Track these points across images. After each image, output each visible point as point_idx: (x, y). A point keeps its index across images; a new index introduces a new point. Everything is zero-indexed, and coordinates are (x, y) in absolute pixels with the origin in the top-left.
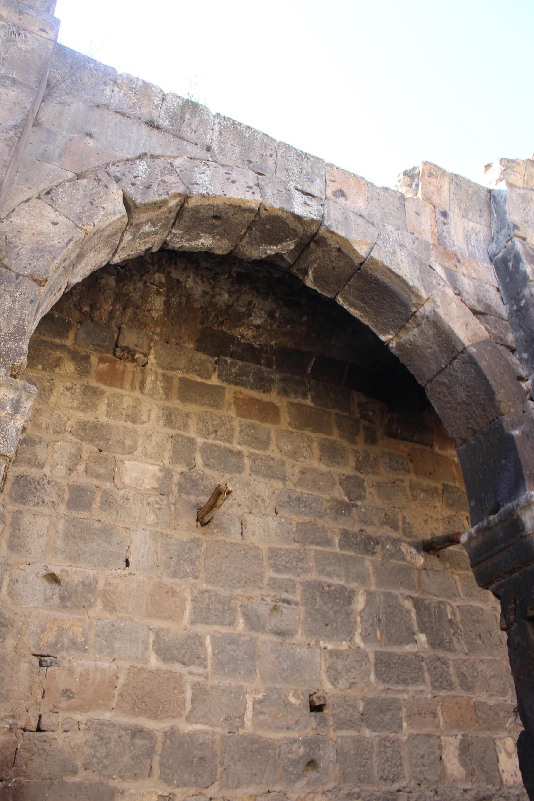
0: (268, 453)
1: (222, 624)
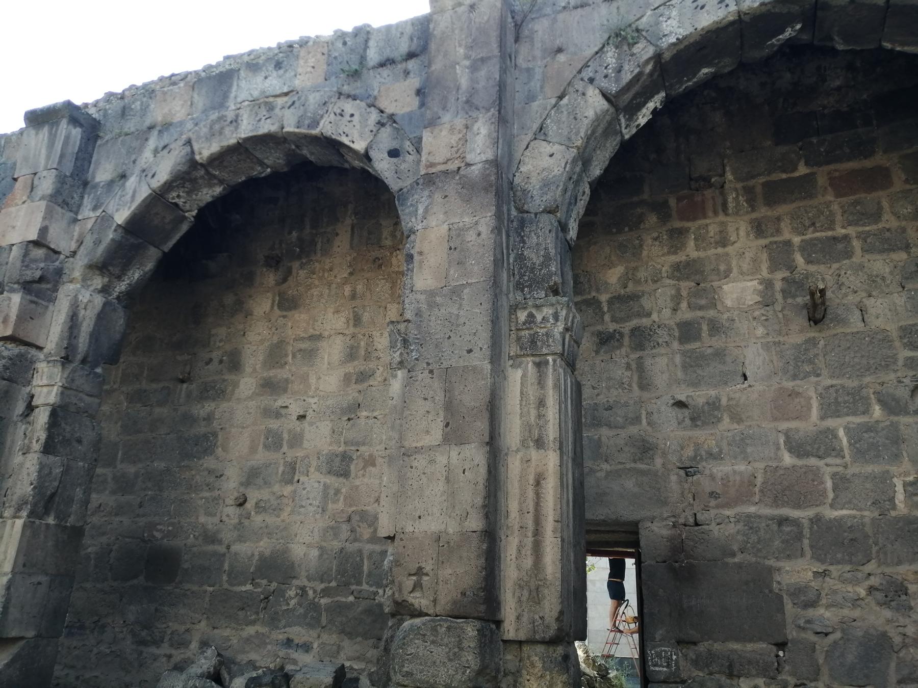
0: (880, 226)
1: (854, 414)
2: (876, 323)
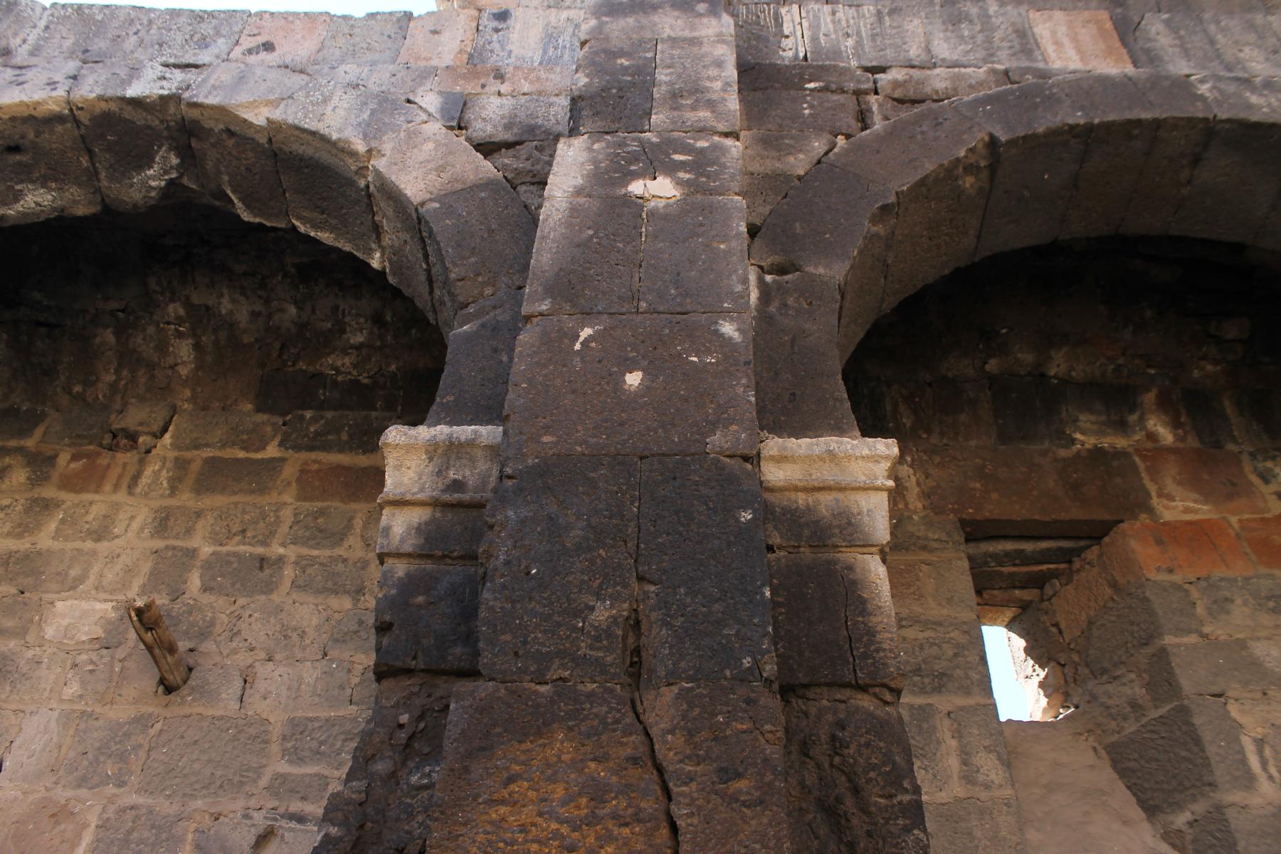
2: (258, 706)
